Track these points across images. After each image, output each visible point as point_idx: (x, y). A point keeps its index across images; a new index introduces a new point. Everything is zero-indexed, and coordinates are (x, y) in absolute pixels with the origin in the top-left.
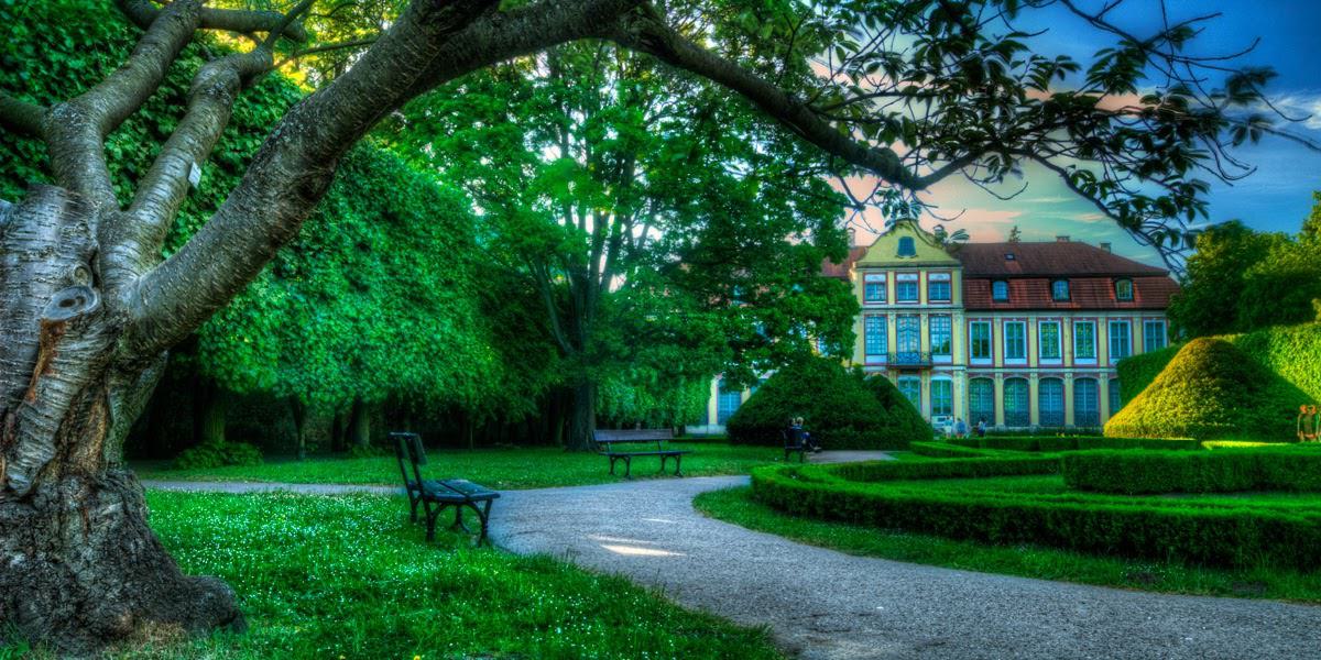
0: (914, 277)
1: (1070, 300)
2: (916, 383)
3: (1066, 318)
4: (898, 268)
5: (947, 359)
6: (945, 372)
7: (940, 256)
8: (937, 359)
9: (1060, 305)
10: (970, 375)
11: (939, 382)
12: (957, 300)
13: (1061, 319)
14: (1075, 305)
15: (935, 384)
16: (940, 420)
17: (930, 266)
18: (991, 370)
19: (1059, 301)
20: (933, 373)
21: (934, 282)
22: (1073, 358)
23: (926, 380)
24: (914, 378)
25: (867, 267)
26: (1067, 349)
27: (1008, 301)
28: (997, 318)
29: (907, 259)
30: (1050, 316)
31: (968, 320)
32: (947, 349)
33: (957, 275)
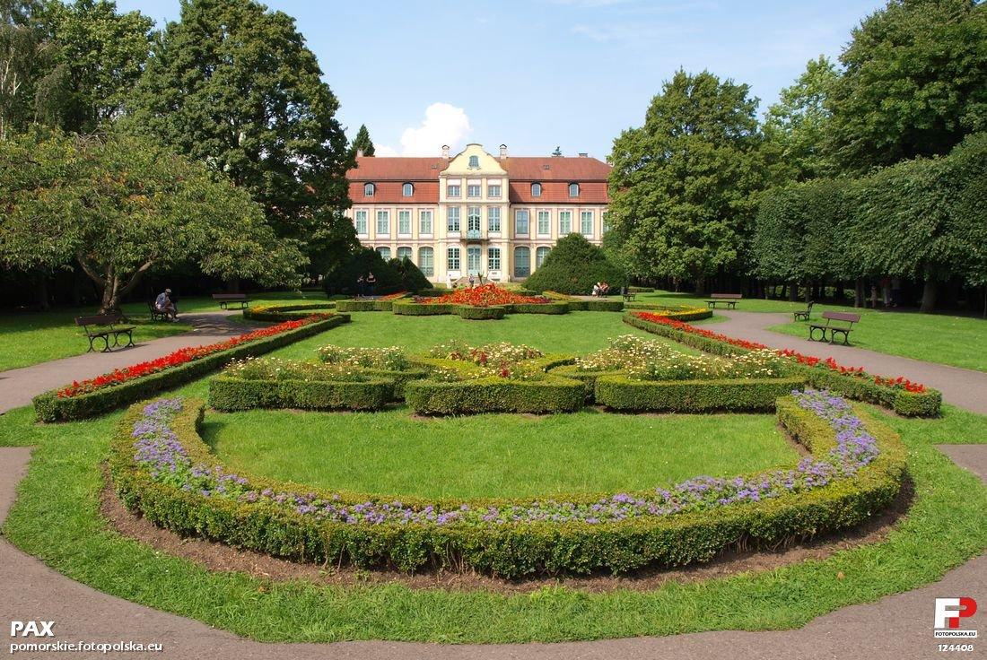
0: (477, 182)
1: (578, 197)
2: (478, 250)
3: (576, 208)
4: (468, 177)
7: (496, 168)
8: (491, 235)
10: (515, 244)
12: (505, 197)
13: (573, 209)
14: (582, 201)
17: (489, 177)
18: (528, 242)
19: (572, 198)
20: (489, 244)
21: (491, 187)
23: (484, 249)
24: (477, 246)
29: (474, 171)
30: (565, 208)
32: (498, 229)
33: (505, 184)
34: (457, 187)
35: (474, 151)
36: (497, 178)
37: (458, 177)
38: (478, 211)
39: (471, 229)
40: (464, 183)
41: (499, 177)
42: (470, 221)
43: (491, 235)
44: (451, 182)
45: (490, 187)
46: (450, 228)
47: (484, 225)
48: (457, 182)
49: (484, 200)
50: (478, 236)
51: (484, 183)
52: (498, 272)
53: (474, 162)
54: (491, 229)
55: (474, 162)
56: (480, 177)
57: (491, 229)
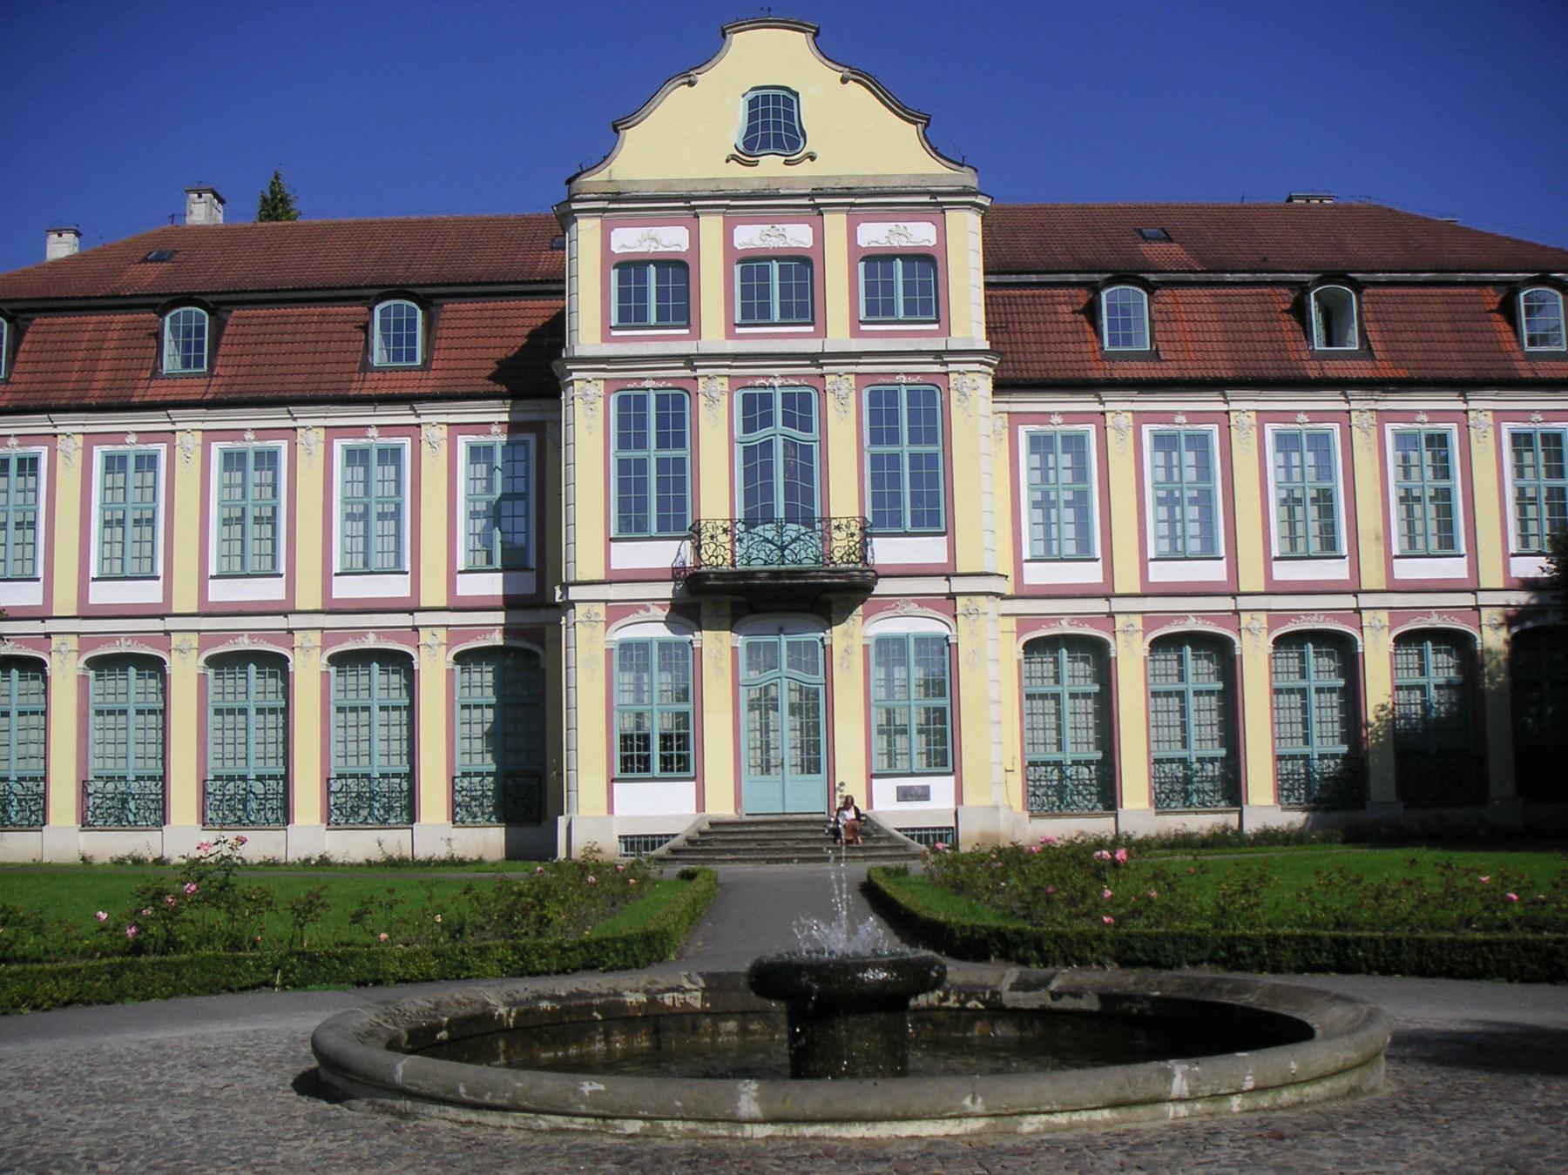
0: (798, 236)
5: (929, 550)
6: (923, 599)
8: (886, 551)
9: (1333, 369)
11: (900, 641)
15: (889, 650)
16: (905, 795)
22: (1390, 558)
25: (617, 197)
26: (1369, 519)
27: (1155, 355)
28: (1120, 408)
29: (771, 167)
31: (1015, 419)
32: (932, 515)
33: (964, 243)
34: (678, 270)
35: (769, 55)
36: (913, 212)
37: (684, 203)
38: (800, 410)
39: (756, 512)
40: (712, 247)
41: (933, 202)
42: (756, 462)
43: (886, 551)
44: (631, 240)
45: (877, 261)
46: (631, 524)
47: (845, 492)
48: (671, 239)
49: (838, 336)
50: (804, 556)
51: (837, 244)
52: (941, 788)
53: (773, 121)
54: (883, 517)
55: (773, 121)
56: (816, 202)
57: (883, 517)
